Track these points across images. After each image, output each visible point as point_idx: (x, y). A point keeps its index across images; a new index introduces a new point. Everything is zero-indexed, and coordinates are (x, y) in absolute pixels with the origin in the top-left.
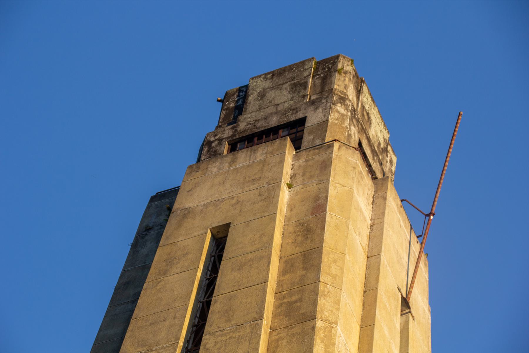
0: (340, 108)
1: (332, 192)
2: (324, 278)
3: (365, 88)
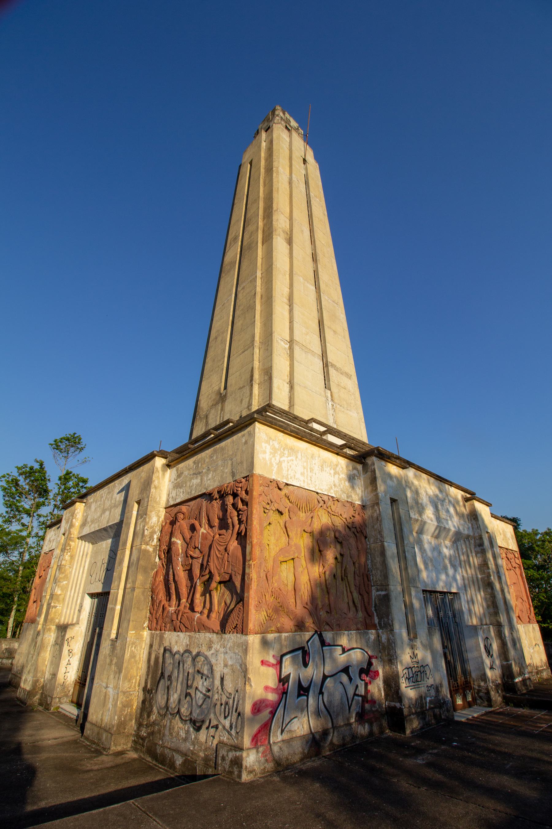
0: (277, 118)
1: (274, 136)
2: (274, 157)
3: (286, 113)
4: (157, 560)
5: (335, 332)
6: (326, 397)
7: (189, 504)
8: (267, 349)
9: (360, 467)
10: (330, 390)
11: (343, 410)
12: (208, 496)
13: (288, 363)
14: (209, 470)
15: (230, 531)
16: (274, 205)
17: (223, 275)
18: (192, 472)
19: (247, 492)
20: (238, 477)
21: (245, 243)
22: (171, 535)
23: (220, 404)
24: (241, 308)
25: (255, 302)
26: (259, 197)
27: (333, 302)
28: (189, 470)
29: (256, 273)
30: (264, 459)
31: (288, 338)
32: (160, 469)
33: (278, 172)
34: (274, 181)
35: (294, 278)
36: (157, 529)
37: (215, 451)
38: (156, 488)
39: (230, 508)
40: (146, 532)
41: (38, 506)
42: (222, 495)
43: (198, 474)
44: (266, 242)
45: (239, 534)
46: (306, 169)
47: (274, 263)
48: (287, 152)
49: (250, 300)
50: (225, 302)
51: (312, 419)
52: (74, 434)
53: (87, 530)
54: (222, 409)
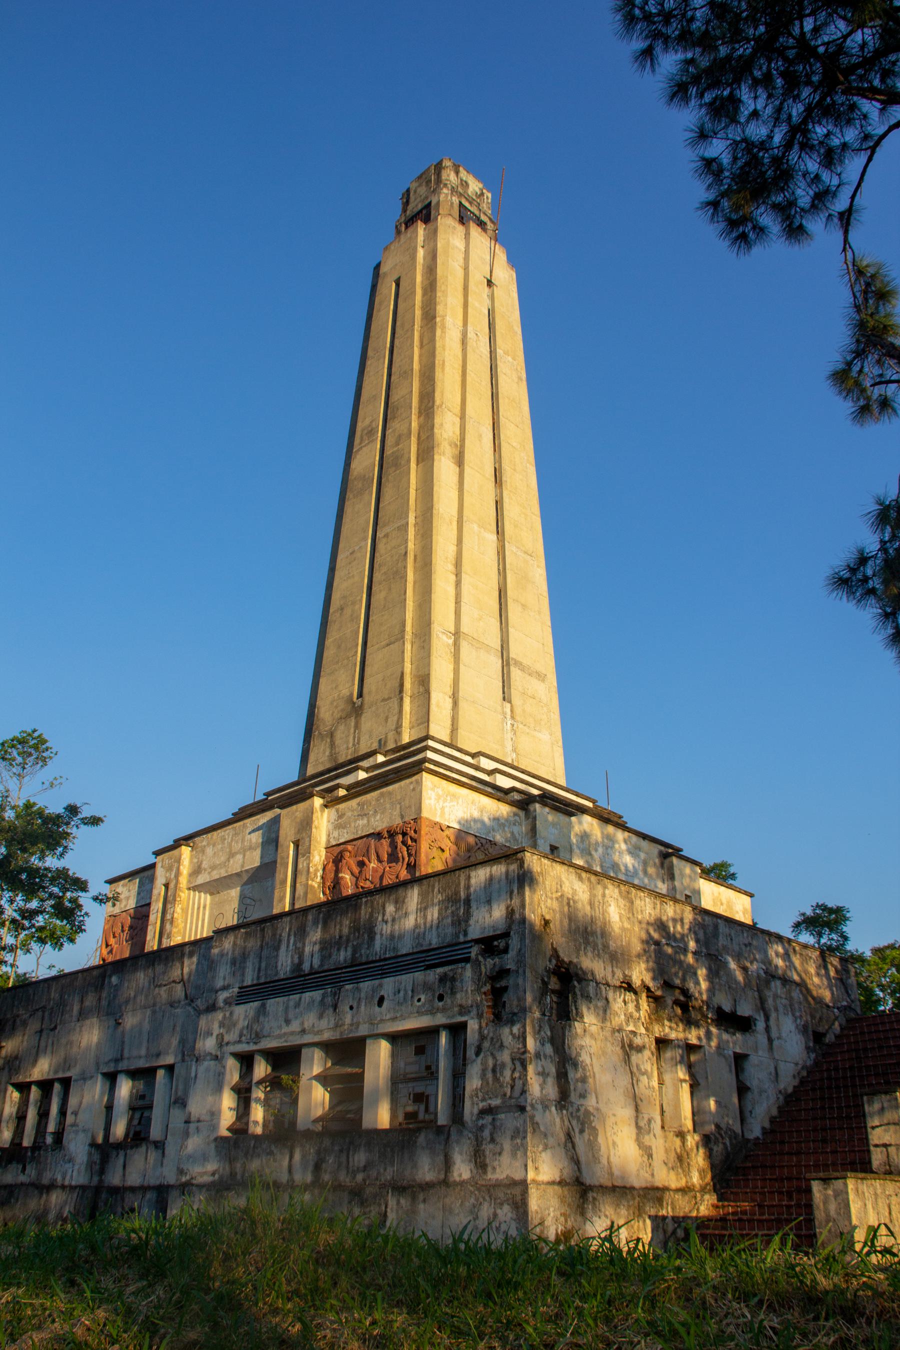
0: (445, 191)
2: (439, 294)
3: (461, 169)
4: (322, 895)
5: (524, 606)
6: (504, 714)
7: (354, 843)
8: (423, 647)
9: (522, 814)
10: (510, 702)
11: (528, 731)
12: (378, 836)
13: (451, 667)
14: (376, 812)
15: (400, 863)
16: (436, 395)
17: (349, 495)
18: (356, 813)
19: (415, 832)
20: (407, 819)
21: (388, 452)
22: (337, 871)
23: (353, 719)
24: (384, 569)
25: (405, 567)
26: (412, 369)
27: (525, 553)
28: (353, 811)
29: (408, 517)
30: (430, 804)
31: (452, 630)
32: (318, 810)
33: (443, 327)
34: (438, 344)
35: (464, 528)
36: (320, 867)
37: (382, 795)
38: (316, 828)
39: (400, 845)
40: (311, 870)
42: (392, 834)
43: (362, 815)
44: (423, 460)
45: (409, 864)
46: (492, 298)
47: (436, 506)
48: (460, 273)
49: (398, 560)
50: (356, 548)
51: (479, 752)
52: (34, 731)
53: (201, 879)
54: (357, 726)
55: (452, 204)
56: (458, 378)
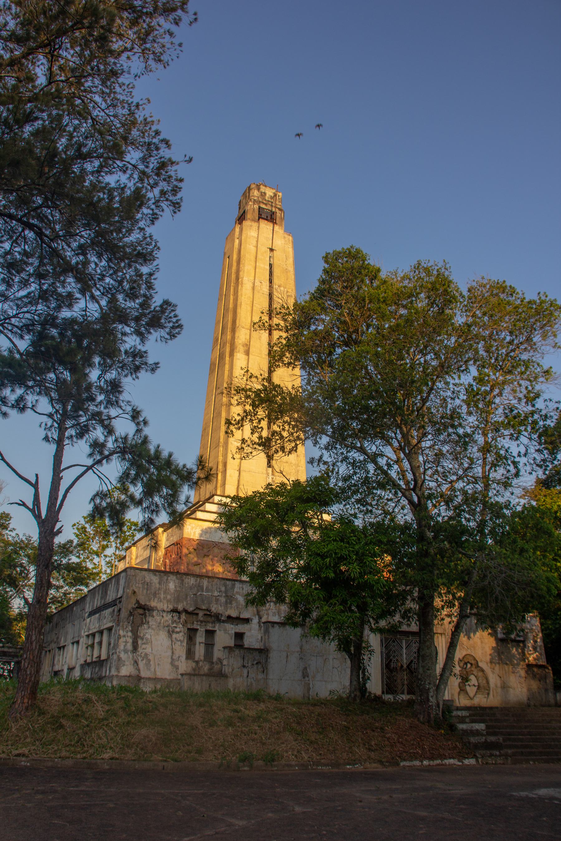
41: (104, 548)
48: (253, 249)
53: (138, 561)
55: (254, 209)
56: (249, 309)
